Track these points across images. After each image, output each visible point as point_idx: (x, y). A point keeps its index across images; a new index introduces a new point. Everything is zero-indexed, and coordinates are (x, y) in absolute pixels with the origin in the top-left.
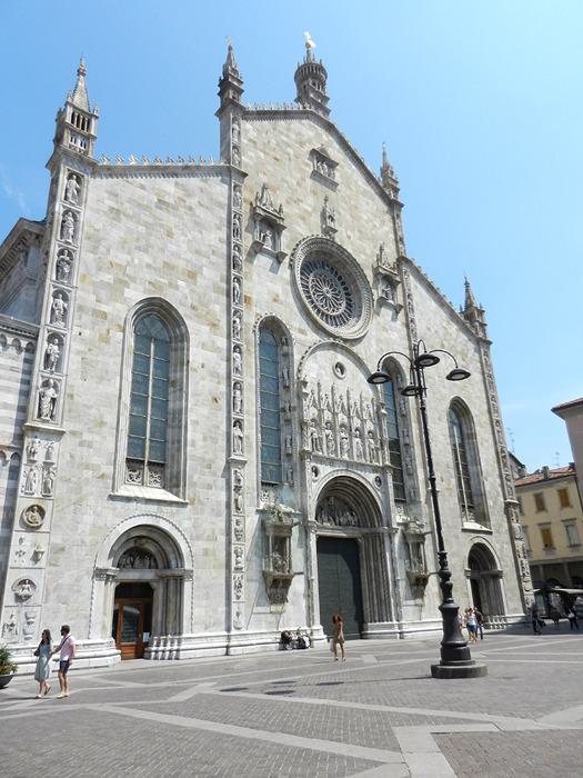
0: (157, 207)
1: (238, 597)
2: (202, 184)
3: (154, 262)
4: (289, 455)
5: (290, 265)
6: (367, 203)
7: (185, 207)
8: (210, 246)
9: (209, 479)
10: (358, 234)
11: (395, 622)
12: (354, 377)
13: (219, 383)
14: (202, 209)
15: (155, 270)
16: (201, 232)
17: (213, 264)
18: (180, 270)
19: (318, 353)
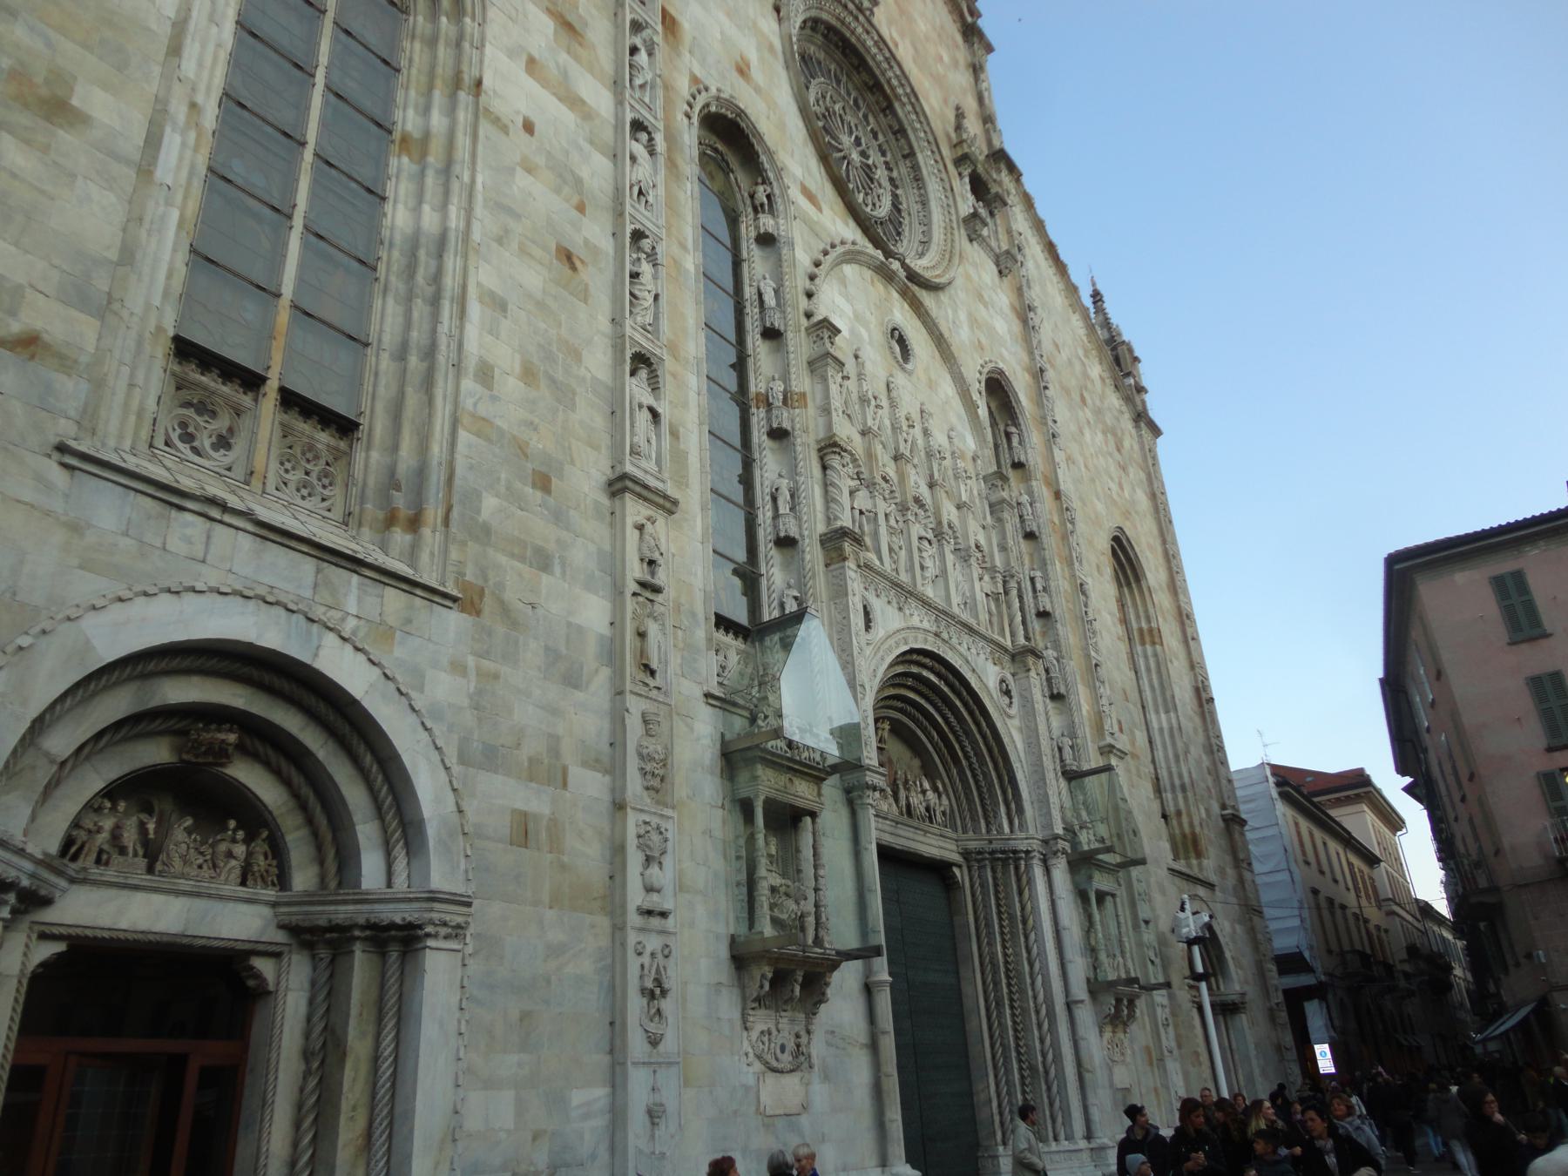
1: (654, 1041)
4: (786, 543)
9: (542, 531)
11: (1083, 1144)
12: (932, 385)
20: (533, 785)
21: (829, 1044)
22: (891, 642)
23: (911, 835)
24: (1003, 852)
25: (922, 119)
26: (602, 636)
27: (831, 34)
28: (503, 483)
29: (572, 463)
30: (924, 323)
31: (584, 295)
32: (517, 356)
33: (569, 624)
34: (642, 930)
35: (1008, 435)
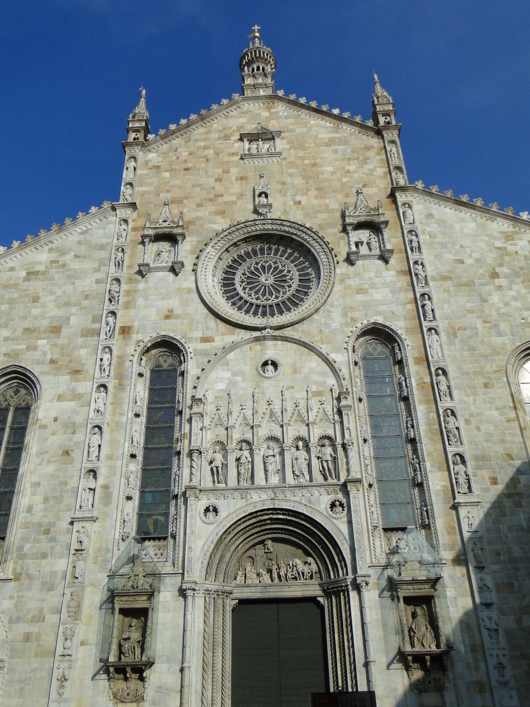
0: (24, 281)
2: (81, 238)
3: (14, 331)
5: (194, 270)
6: (336, 152)
7: (57, 268)
8: (82, 292)
9: (45, 546)
10: (313, 193)
13: (74, 433)
14: (78, 259)
15: (13, 339)
16: (74, 283)
17: (85, 307)
18: (42, 329)
19: (231, 356)
20: (32, 624)
21: (156, 691)
22: (234, 516)
23: (278, 590)
24: (337, 587)
25: (309, 232)
26: (64, 571)
27: (247, 240)
28: (33, 538)
29: (60, 520)
30: (295, 343)
31: (72, 462)
32: (42, 497)
33: (52, 572)
34: (60, 661)
35: (393, 348)
